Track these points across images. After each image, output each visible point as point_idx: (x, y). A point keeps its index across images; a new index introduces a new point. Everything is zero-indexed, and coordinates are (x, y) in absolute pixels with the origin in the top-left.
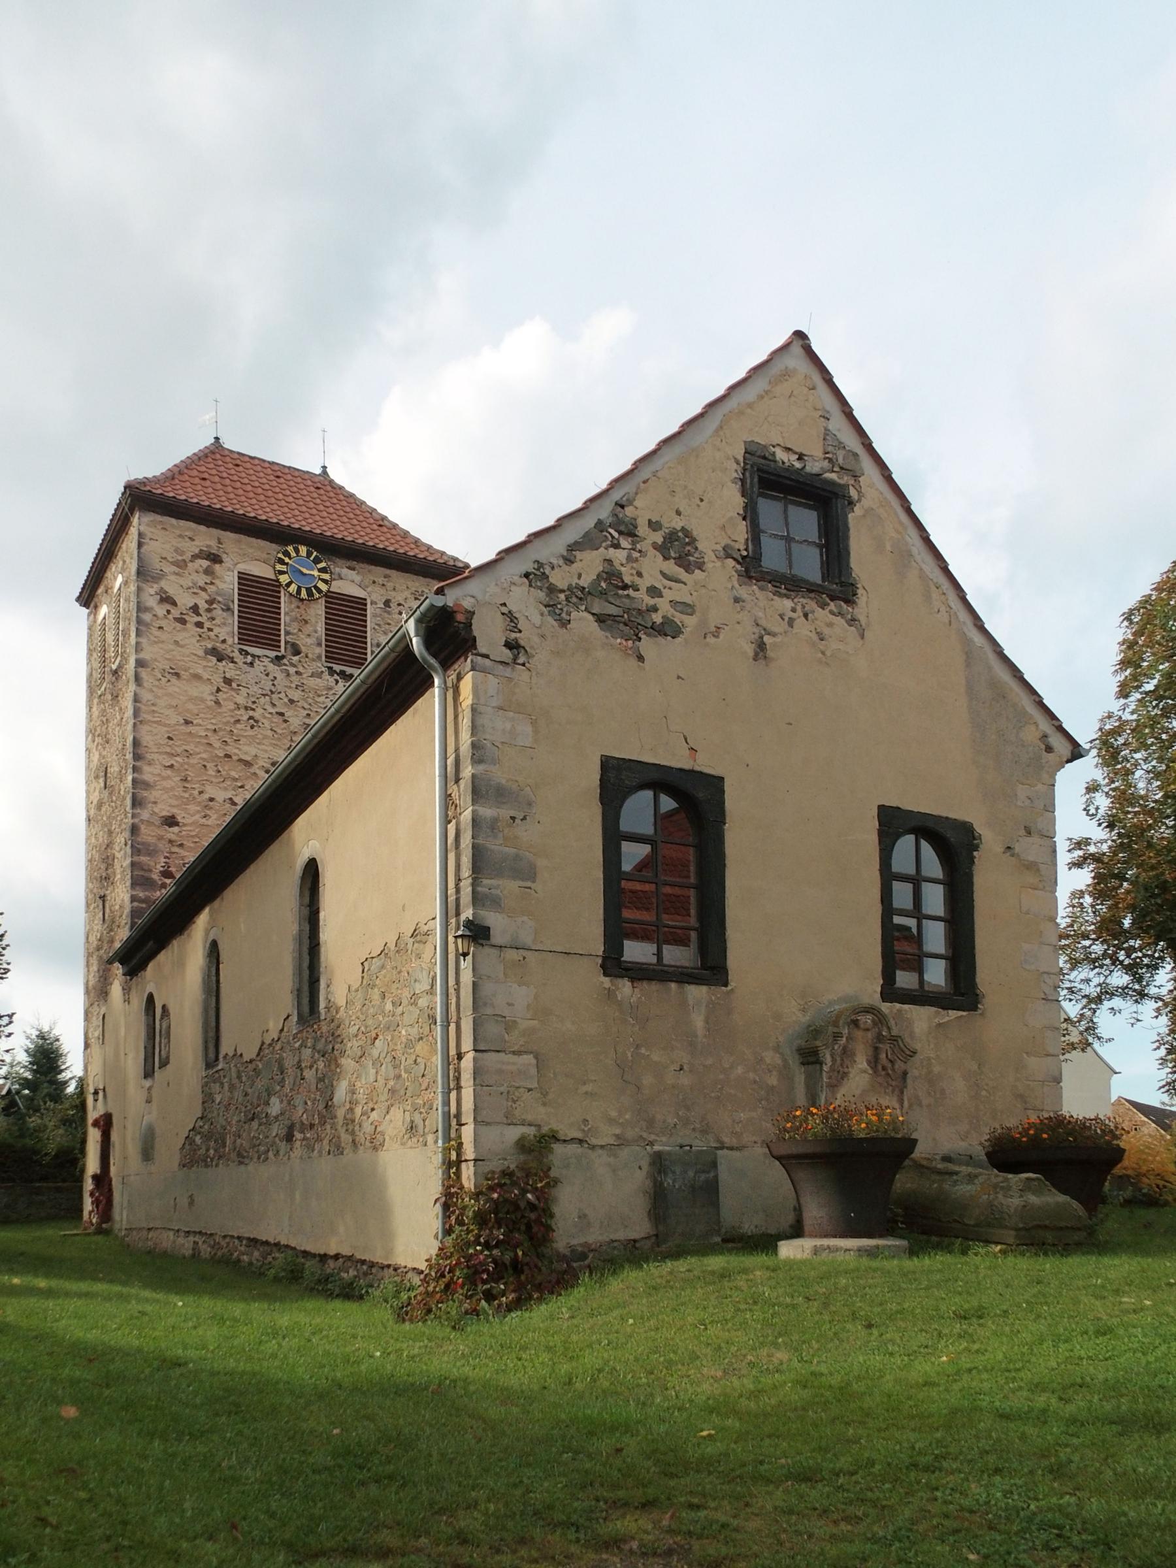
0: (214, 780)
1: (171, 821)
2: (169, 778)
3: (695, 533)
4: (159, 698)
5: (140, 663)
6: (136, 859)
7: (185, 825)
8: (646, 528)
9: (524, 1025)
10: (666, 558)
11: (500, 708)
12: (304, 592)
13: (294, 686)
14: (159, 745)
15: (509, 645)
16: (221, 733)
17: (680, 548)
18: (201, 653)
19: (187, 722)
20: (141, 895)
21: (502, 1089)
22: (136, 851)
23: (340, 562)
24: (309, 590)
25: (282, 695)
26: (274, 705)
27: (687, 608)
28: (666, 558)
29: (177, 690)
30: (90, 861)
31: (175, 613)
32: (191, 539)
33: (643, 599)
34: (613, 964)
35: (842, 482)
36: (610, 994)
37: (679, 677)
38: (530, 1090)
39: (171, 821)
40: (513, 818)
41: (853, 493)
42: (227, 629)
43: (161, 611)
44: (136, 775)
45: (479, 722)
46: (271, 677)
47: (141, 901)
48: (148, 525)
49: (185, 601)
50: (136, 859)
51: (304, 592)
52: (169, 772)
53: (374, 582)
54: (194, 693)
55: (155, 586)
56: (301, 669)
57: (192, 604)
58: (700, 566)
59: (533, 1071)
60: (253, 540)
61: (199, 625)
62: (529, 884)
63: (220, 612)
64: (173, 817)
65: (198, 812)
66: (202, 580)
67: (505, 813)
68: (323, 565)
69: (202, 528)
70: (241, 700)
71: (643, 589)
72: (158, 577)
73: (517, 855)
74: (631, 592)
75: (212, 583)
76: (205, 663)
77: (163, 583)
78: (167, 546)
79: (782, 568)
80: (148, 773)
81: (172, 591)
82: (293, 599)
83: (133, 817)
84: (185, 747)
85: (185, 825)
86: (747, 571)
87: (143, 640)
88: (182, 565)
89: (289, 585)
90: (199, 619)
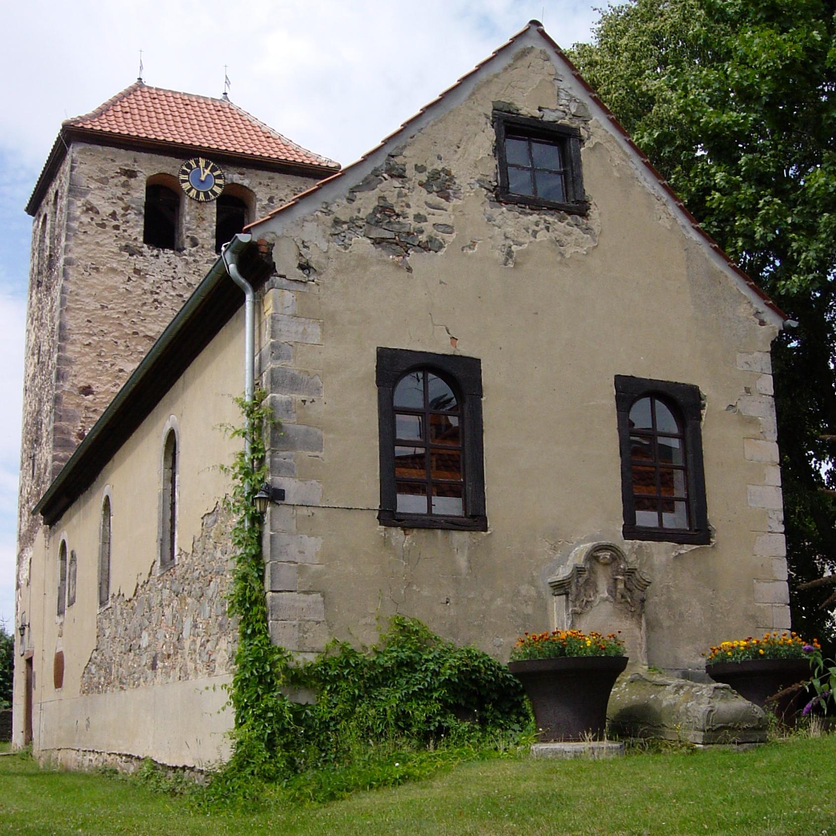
0: (122, 353)
1: (87, 390)
2: (87, 354)
3: (453, 172)
4: (82, 289)
5: (68, 262)
6: (58, 424)
7: (99, 393)
8: (413, 171)
10: (430, 192)
12: (202, 195)
13: (191, 272)
14: (79, 328)
16: (130, 315)
17: (441, 184)
18: (116, 250)
19: (103, 307)
22: (59, 418)
23: (232, 169)
24: (206, 195)
25: (182, 280)
26: (174, 288)
27: (448, 229)
29: (95, 281)
30: (26, 424)
31: (98, 220)
33: (410, 223)
34: (389, 516)
39: (87, 390)
40: (304, 401)
43: (85, 219)
44: (60, 353)
46: (173, 266)
49: (106, 209)
50: (58, 424)
51: (202, 195)
52: (87, 349)
53: (260, 183)
54: (110, 283)
56: (198, 258)
57: (111, 211)
61: (116, 227)
62: (317, 453)
64: (89, 387)
65: (110, 382)
66: (119, 192)
67: (298, 397)
68: (218, 172)
69: (122, 151)
70: (147, 286)
71: (411, 217)
72: (84, 193)
73: (307, 431)
75: (128, 194)
76: (119, 258)
77: (89, 197)
78: (94, 168)
80: (71, 351)
81: (95, 203)
82: (193, 202)
83: (57, 388)
84: (101, 328)
85: (99, 393)
86: (497, 196)
87: (71, 243)
88: (104, 181)
89: (189, 191)
90: (116, 223)
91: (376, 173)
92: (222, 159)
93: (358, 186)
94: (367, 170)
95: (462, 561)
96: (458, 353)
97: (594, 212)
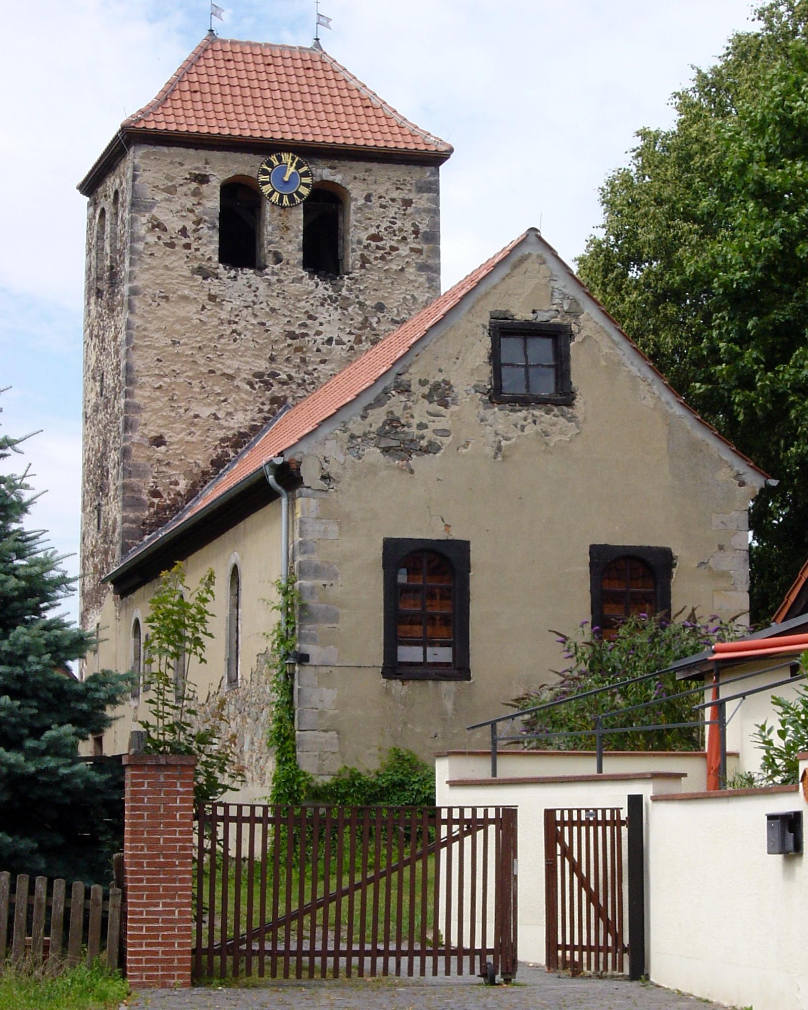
0: (198, 396)
1: (159, 441)
2: (158, 399)
3: (452, 382)
4: (150, 322)
5: (134, 292)
6: (127, 481)
7: (172, 444)
8: (418, 385)
9: (331, 712)
10: (431, 402)
11: (318, 518)
12: (286, 199)
13: (275, 294)
14: (148, 368)
15: (323, 478)
16: (205, 350)
17: (441, 394)
18: (188, 273)
19: (174, 343)
20: (131, 515)
21: (316, 753)
22: (128, 473)
23: (321, 163)
24: (291, 197)
25: (264, 305)
26: (255, 316)
27: (445, 433)
28: (431, 402)
29: (165, 312)
30: (88, 460)
31: (166, 238)
32: (181, 164)
33: (414, 431)
34: (393, 669)
35: (565, 323)
36: (387, 691)
37: (438, 480)
38: (333, 753)
39: (159, 441)
40: (325, 585)
41: (574, 328)
42: (210, 247)
43: (151, 239)
44: (128, 399)
45: (304, 529)
46: (253, 288)
47: (133, 522)
48: (141, 157)
49: (174, 224)
50: (127, 481)
51: (286, 199)
52: (158, 393)
53: (355, 178)
54: (182, 314)
55: (147, 215)
56: (282, 277)
57: (181, 227)
58: (455, 403)
59: (336, 741)
60: (238, 155)
61: (187, 246)
62: (334, 625)
63: (207, 231)
64: (161, 437)
65: (184, 429)
66: (189, 202)
67: (320, 582)
68: (305, 169)
69: (192, 152)
70: (224, 315)
71: (415, 426)
72: (149, 207)
73: (327, 608)
74: (406, 429)
75: (199, 204)
76: (191, 283)
77: (155, 211)
78: (159, 175)
79: (521, 391)
80: (140, 396)
81: (162, 218)
82: (276, 208)
83: (125, 440)
84: (172, 367)
85: (172, 444)
86: (490, 398)
87: (136, 269)
88: (171, 190)
89: (271, 195)
90: (186, 241)
91: (386, 392)
92: (308, 152)
93: (370, 405)
94: (379, 389)
95: (449, 705)
96: (450, 538)
97: (579, 402)
